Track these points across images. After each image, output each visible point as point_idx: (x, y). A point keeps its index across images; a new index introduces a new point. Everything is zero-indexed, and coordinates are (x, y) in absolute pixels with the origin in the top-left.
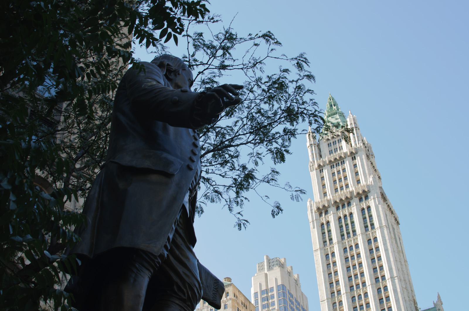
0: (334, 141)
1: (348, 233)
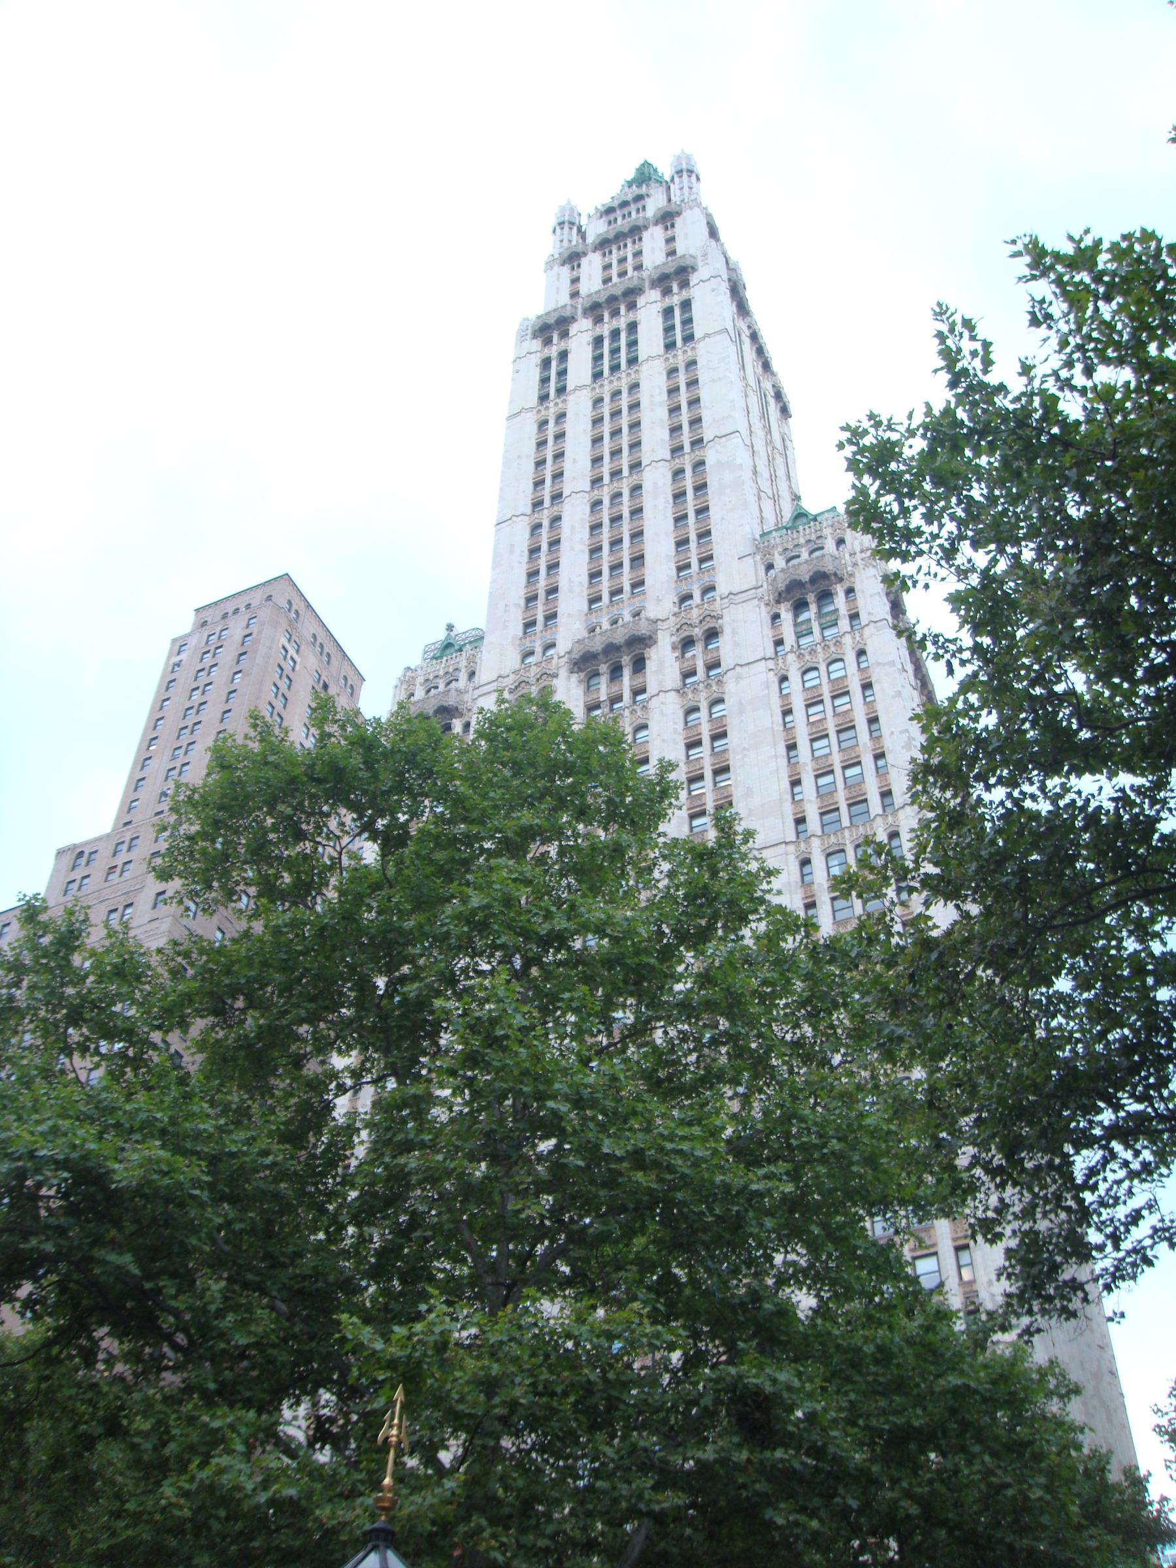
1: (615, 368)
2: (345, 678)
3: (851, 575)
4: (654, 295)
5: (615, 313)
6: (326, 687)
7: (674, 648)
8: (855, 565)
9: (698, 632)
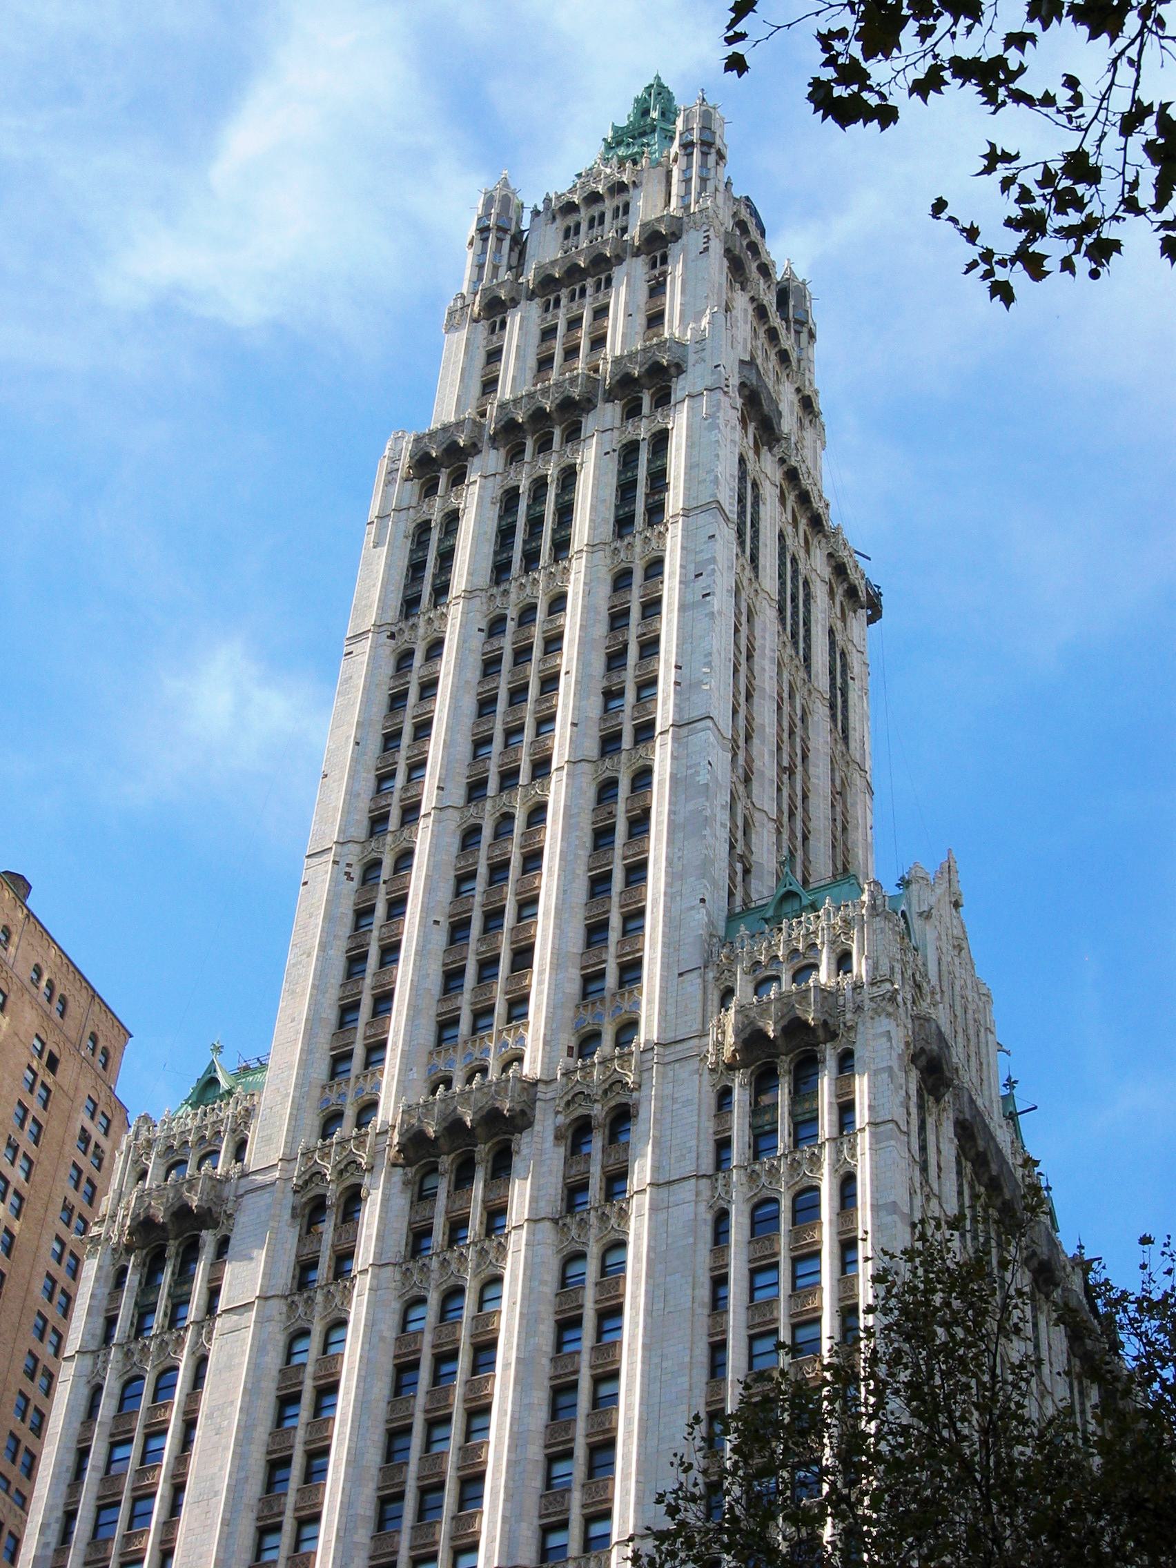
0: (596, 214)
1: (531, 558)
2: (94, 1038)
3: (850, 1028)
4: (609, 413)
5: (544, 446)
6: (53, 1064)
7: (558, 1137)
8: (858, 1009)
9: (598, 1111)
